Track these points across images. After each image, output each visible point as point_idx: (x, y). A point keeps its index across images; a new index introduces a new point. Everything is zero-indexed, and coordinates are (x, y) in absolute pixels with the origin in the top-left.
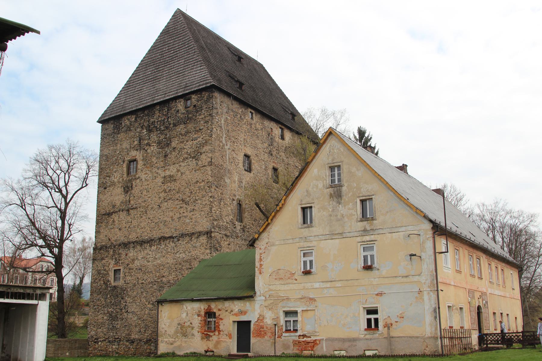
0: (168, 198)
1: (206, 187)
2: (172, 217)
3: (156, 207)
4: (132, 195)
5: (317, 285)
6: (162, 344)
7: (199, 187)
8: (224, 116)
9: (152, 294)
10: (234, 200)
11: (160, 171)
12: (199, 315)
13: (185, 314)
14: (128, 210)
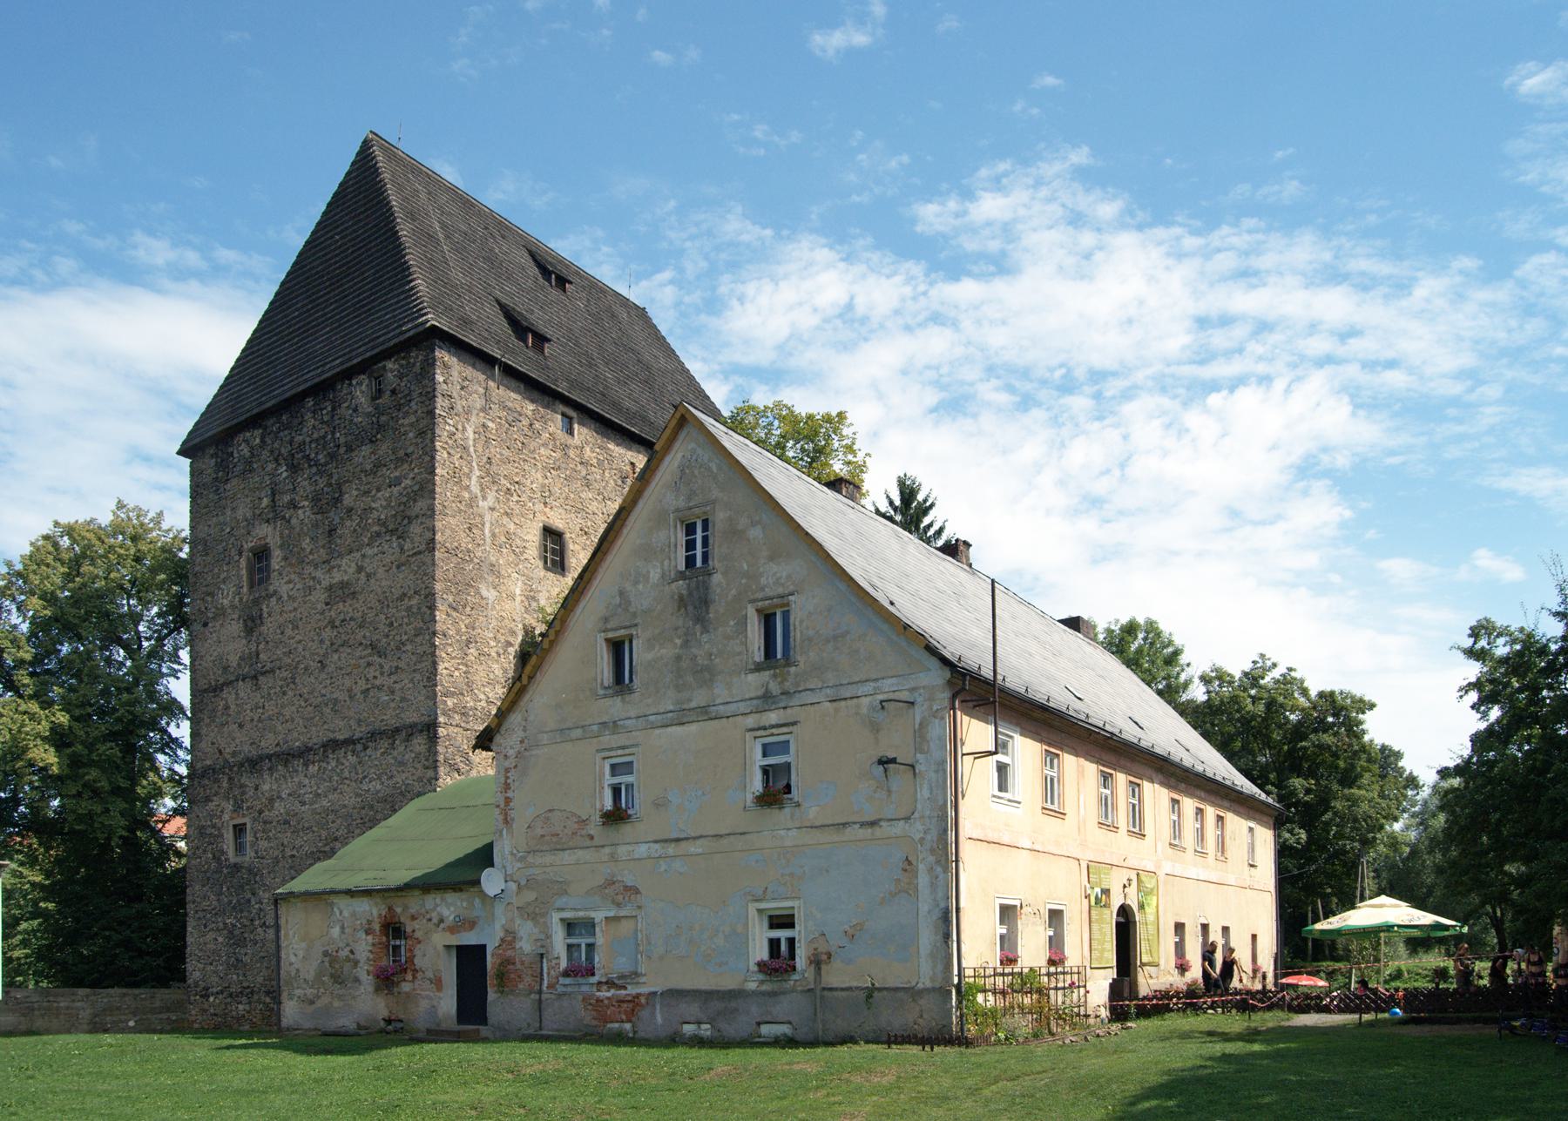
0: (339, 642)
3: (314, 665)
5: (643, 850)
7: (409, 609)
8: (473, 419)
10: (510, 644)
11: (319, 574)
12: (367, 933)
13: (336, 931)
14: (255, 677)
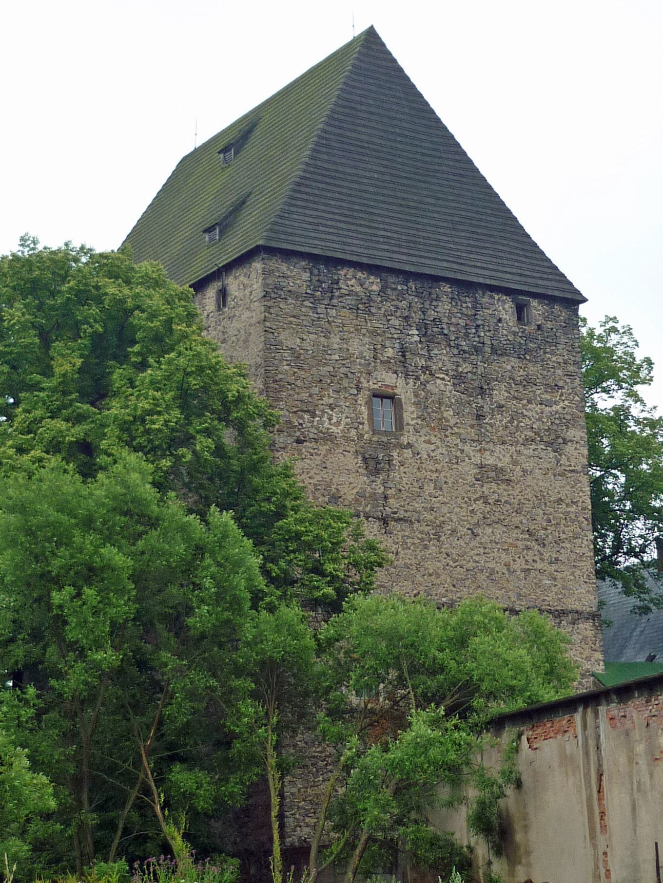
1: (581, 518)
2: (507, 565)
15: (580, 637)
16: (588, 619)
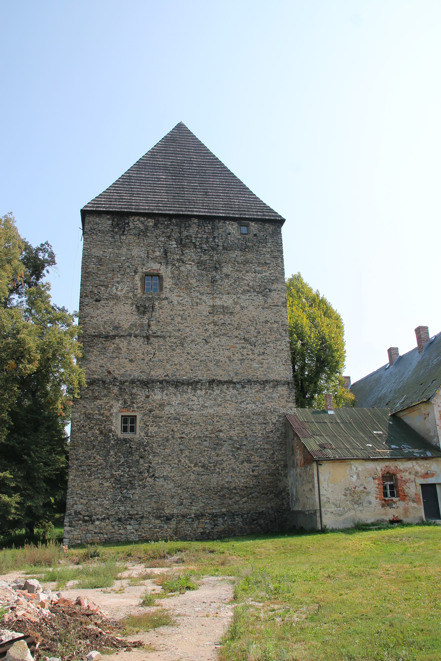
1: (281, 330)
2: (229, 358)
4: (153, 319)
6: (326, 516)
9: (201, 453)
14: (148, 338)
15: (279, 395)
16: (284, 384)
